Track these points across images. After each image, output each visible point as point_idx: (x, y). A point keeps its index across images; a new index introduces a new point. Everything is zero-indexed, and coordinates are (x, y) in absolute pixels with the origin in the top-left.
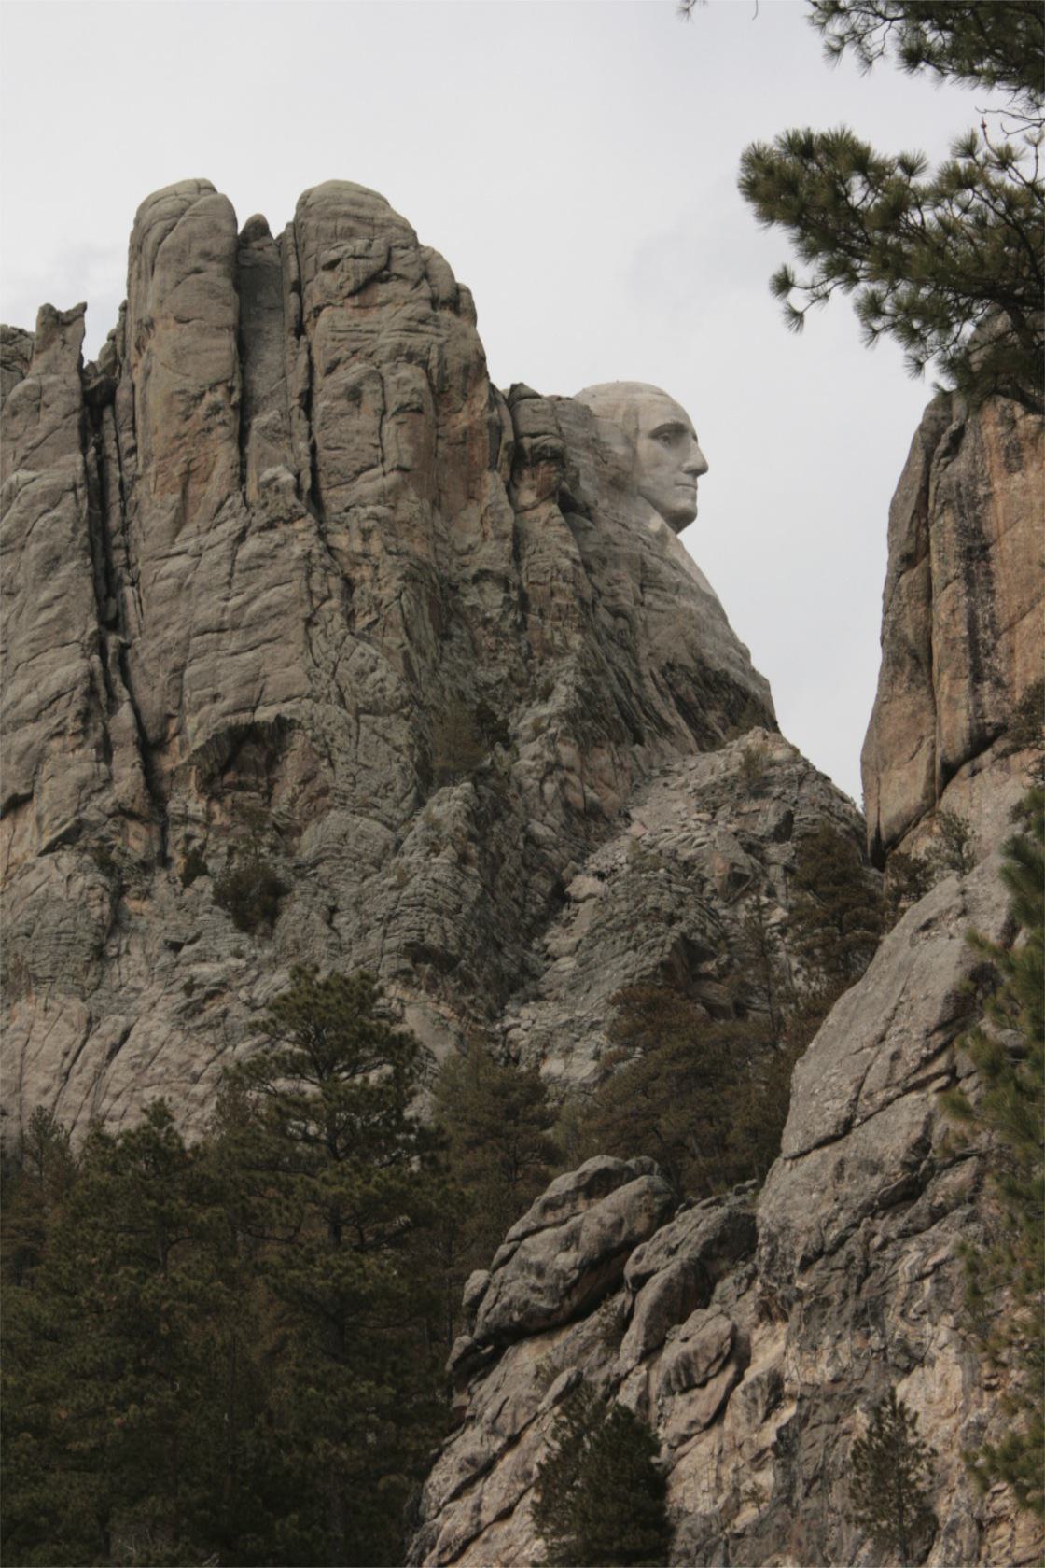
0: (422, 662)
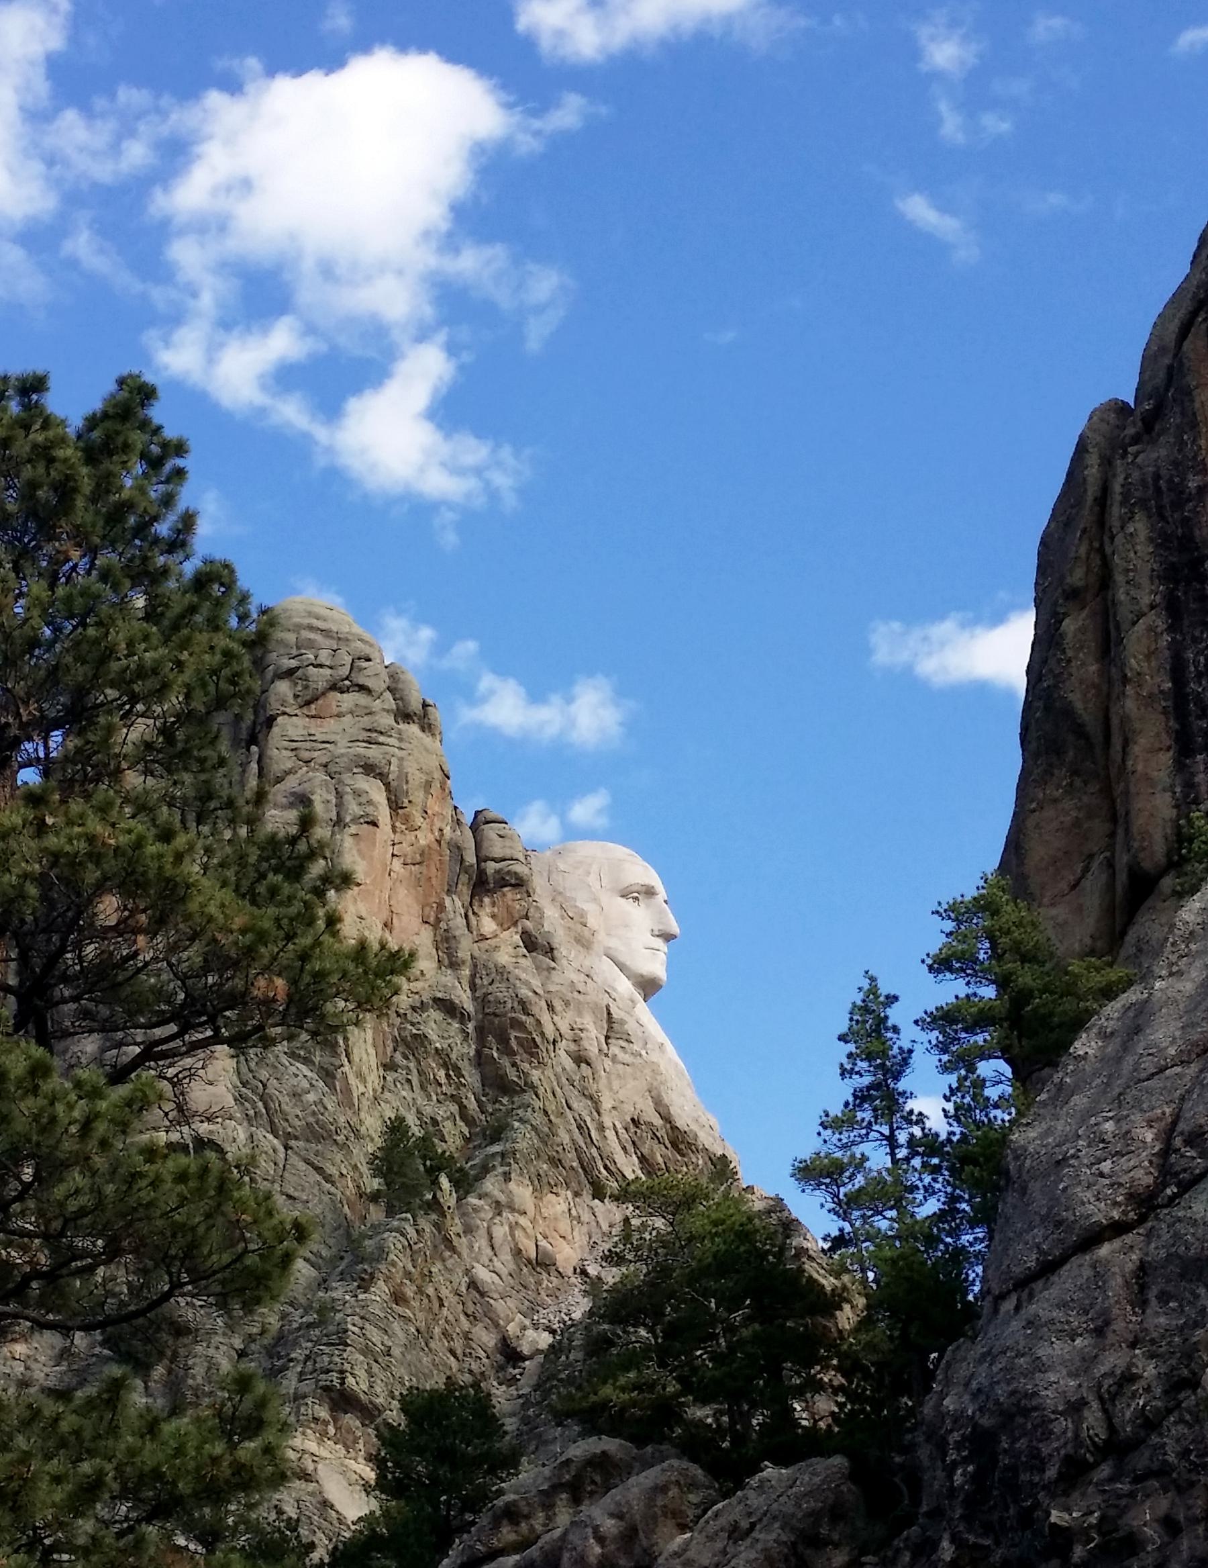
0: (362, 1089)
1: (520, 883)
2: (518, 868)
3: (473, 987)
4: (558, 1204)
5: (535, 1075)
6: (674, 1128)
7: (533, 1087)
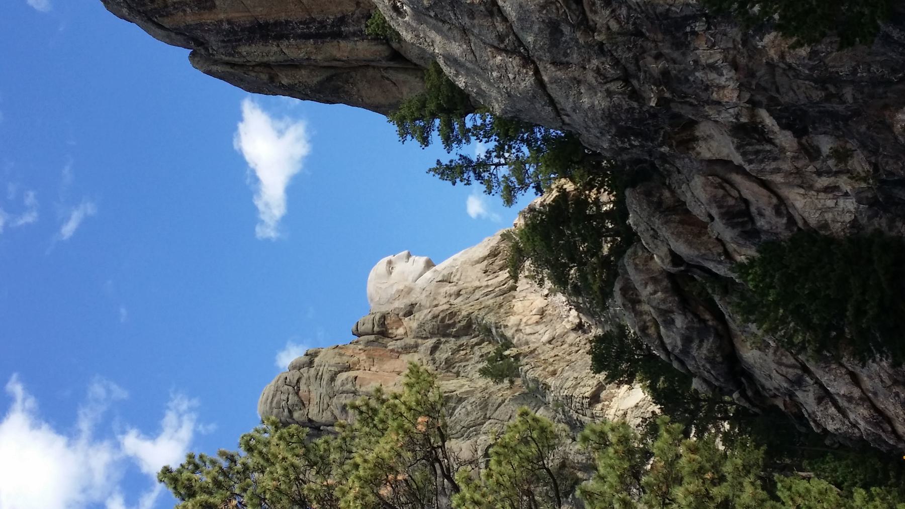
1: (384, 317)
3: (426, 338)
4: (518, 305)
5: (464, 313)
6: (489, 256)
7: (469, 314)
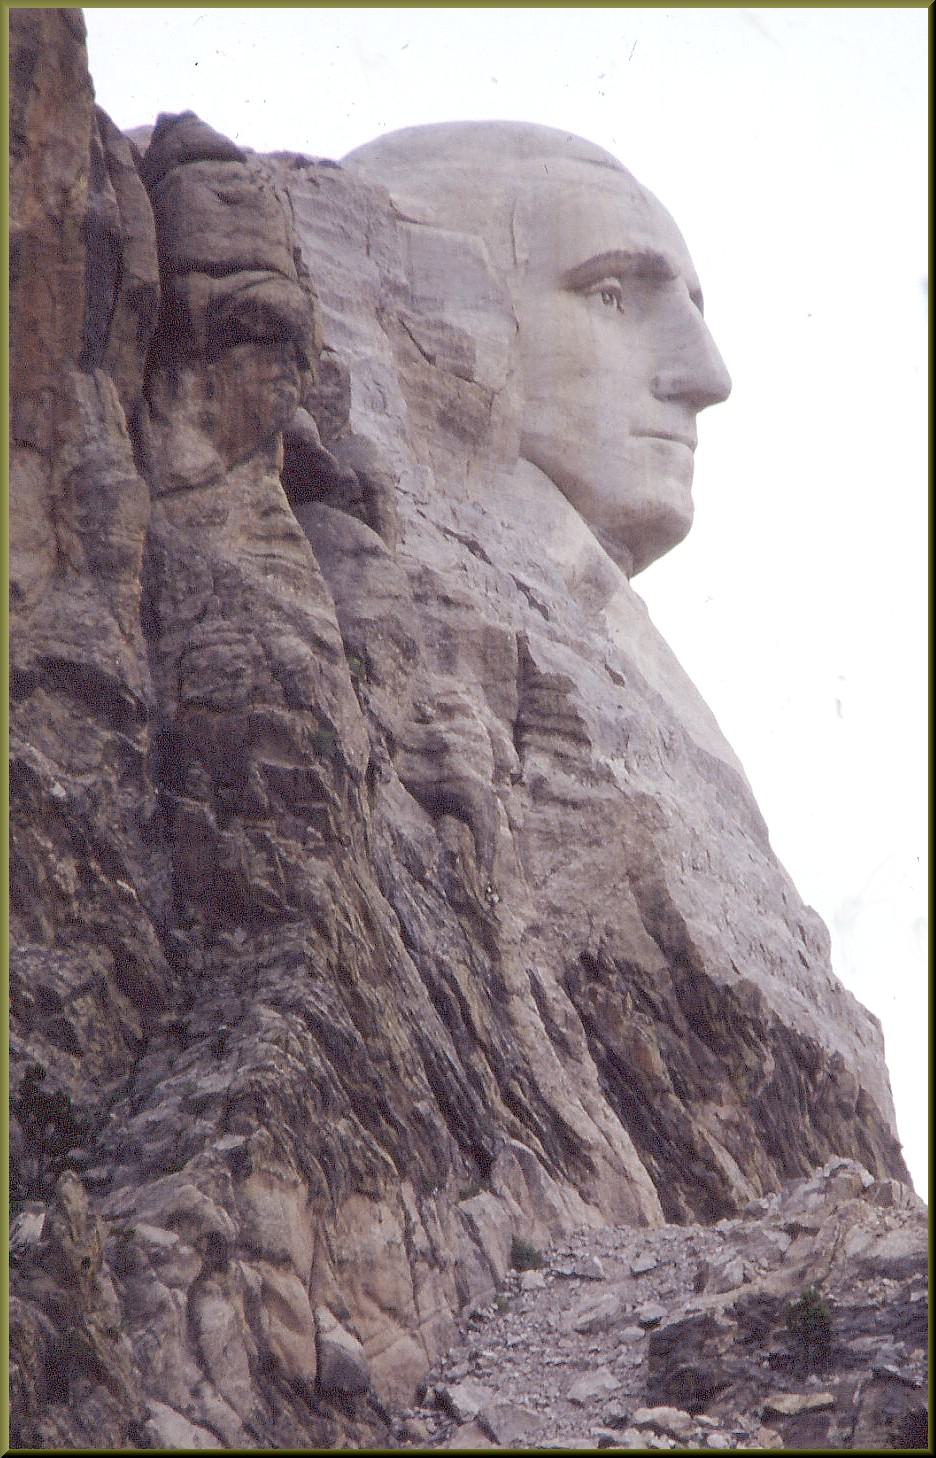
2: (272, 292)
3: (153, 624)
4: (376, 1228)
5: (318, 873)
